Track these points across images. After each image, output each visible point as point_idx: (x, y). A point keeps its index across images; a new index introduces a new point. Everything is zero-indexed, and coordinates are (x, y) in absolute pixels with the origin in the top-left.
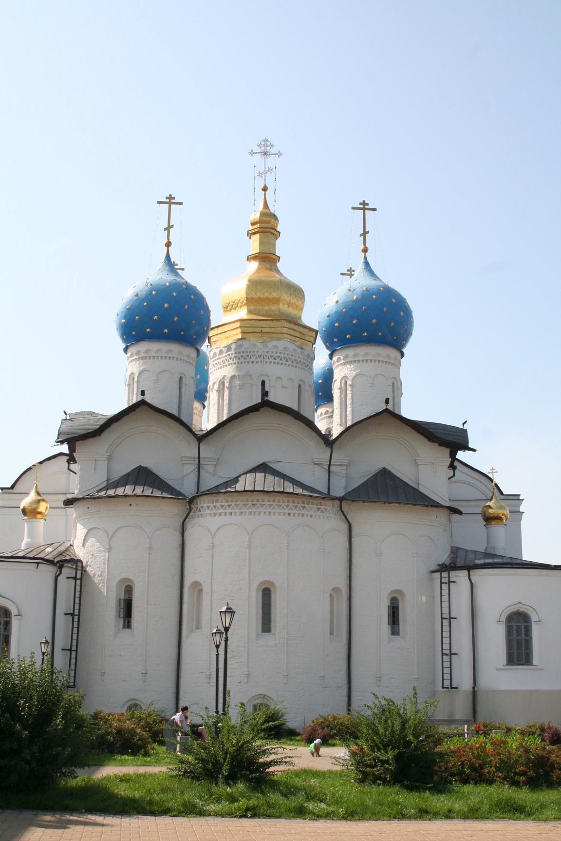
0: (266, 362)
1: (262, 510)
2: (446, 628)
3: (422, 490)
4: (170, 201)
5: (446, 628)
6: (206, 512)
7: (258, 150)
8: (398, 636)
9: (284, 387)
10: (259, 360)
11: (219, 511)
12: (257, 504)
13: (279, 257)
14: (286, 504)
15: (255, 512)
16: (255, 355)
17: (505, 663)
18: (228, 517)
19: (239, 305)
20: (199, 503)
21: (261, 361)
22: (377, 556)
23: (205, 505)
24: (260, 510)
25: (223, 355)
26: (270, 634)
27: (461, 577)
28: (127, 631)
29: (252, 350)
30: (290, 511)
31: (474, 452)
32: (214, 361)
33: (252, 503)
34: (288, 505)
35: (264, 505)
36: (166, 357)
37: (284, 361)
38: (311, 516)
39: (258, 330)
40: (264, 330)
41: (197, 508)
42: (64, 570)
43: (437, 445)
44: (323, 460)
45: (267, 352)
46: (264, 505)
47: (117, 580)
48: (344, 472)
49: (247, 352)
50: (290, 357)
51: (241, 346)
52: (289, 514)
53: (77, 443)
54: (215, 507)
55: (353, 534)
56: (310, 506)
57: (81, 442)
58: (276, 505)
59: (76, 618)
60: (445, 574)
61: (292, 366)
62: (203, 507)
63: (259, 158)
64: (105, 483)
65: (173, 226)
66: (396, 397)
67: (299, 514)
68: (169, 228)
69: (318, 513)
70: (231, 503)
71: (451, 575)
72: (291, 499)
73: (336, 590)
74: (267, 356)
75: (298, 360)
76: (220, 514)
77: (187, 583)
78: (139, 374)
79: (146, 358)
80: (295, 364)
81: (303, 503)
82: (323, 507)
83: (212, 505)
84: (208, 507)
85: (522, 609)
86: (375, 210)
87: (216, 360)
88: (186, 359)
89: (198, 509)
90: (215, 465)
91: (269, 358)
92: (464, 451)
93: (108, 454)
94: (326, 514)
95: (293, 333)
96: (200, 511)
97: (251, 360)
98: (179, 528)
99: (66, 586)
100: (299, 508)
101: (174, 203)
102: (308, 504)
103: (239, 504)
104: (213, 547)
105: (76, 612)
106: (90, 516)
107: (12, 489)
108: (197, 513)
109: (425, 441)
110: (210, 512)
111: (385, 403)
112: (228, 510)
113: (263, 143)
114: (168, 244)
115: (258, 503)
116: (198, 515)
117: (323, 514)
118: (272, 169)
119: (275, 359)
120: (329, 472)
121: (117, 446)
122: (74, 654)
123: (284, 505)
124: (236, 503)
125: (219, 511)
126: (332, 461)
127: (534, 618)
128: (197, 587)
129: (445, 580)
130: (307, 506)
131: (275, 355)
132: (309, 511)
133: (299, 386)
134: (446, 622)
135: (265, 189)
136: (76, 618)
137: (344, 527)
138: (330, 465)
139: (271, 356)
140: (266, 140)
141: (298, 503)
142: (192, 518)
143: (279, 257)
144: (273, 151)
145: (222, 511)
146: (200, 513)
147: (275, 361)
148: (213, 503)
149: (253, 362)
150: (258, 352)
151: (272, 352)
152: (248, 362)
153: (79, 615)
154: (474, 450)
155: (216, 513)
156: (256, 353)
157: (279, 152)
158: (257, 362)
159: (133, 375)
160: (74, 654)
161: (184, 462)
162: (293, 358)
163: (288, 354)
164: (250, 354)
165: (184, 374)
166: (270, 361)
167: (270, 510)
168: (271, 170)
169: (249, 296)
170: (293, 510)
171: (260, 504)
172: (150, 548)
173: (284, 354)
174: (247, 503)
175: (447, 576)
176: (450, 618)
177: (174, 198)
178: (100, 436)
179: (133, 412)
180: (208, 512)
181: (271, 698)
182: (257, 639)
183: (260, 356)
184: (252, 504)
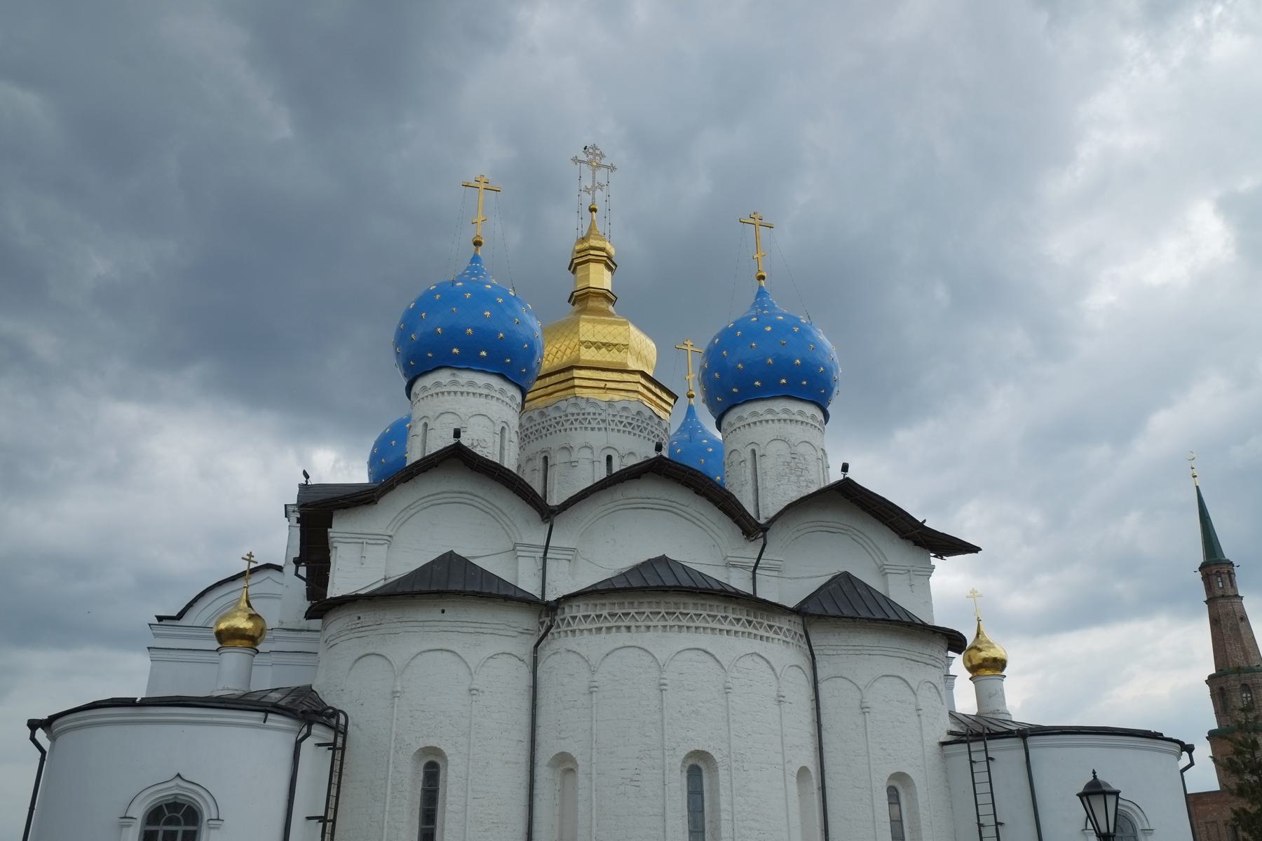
0: (613, 430)
1: (685, 622)
6: (581, 627)
7: (583, 157)
10: (602, 425)
12: (675, 613)
13: (617, 298)
14: (724, 615)
15: (671, 627)
16: (596, 419)
18: (623, 638)
20: (567, 610)
21: (606, 429)
22: (864, 713)
23: (580, 615)
24: (681, 624)
25: (544, 420)
27: (1007, 754)
31: (974, 555)
33: (666, 611)
35: (688, 614)
37: (637, 432)
39: (602, 384)
40: (610, 385)
41: (563, 620)
43: (911, 543)
44: (743, 560)
45: (614, 416)
46: (688, 614)
52: (728, 631)
54: (599, 616)
56: (759, 620)
58: (709, 615)
59: (329, 825)
67: (743, 633)
69: (771, 634)
72: (731, 607)
73: (803, 771)
75: (656, 432)
76: (609, 629)
77: (544, 757)
80: (651, 437)
88: (507, 400)
89: (566, 621)
90: (570, 561)
91: (616, 424)
92: (942, 559)
93: (391, 534)
94: (781, 636)
95: (645, 392)
97: (589, 426)
98: (528, 658)
99: (315, 762)
100: (743, 623)
105: (330, 816)
106: (360, 635)
107: (179, 620)
108: (563, 628)
110: (590, 627)
111: (842, 471)
112: (627, 622)
115: (678, 611)
116: (566, 632)
118: (603, 186)
119: (624, 426)
123: (720, 614)
125: (608, 625)
126: (761, 561)
128: (566, 764)
129: (983, 756)
131: (625, 421)
136: (329, 825)
138: (756, 568)
143: (617, 298)
144: (603, 162)
146: (570, 629)
147: (625, 429)
149: (593, 429)
150: (600, 414)
151: (621, 416)
152: (586, 428)
153: (334, 821)
154: (975, 549)
156: (597, 416)
157: (612, 164)
158: (600, 429)
159: (424, 421)
161: (519, 553)
164: (589, 417)
165: (508, 426)
166: (619, 428)
167: (698, 624)
171: (681, 613)
174: (659, 610)
183: (604, 421)
184: (667, 613)
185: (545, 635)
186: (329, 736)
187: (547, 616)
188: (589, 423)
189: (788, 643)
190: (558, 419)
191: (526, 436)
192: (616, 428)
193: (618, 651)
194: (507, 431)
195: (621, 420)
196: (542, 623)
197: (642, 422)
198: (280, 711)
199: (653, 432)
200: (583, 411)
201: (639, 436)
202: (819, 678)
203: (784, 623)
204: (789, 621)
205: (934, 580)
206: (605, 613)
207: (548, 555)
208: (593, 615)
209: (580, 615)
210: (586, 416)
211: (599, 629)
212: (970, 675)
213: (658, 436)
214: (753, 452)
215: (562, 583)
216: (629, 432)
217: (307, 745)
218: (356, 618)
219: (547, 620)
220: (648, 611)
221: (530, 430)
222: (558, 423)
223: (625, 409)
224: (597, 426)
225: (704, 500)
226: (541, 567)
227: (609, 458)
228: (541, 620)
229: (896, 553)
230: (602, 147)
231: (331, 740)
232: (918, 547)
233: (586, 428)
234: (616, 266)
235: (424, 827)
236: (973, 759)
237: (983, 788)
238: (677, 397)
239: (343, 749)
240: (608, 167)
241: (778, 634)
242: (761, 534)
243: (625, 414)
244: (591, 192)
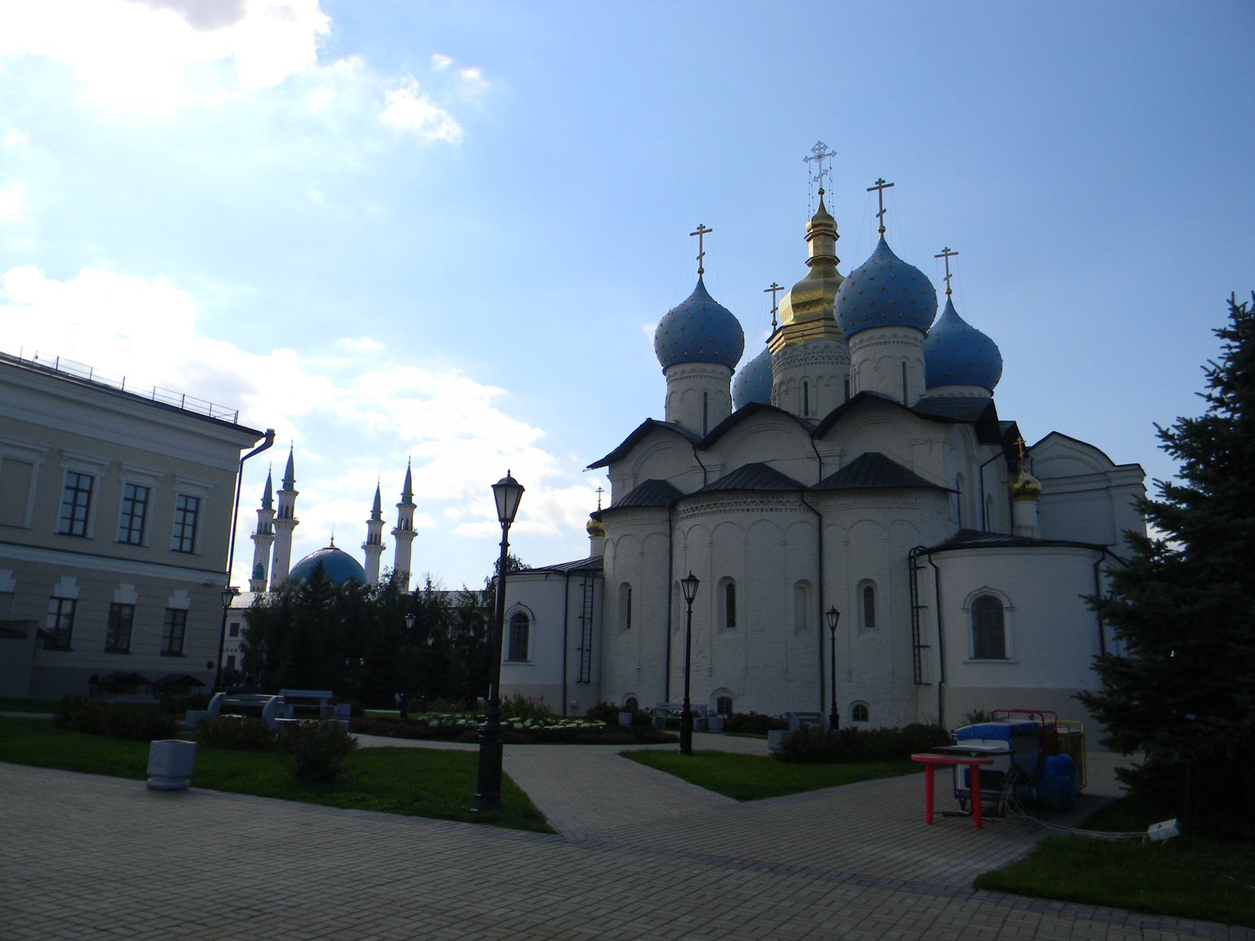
3: (918, 472)
8: (873, 629)
9: (827, 385)
10: (801, 362)
14: (745, 500)
15: (716, 512)
17: (972, 655)
18: (697, 520)
26: (733, 628)
29: (795, 355)
30: (748, 507)
34: (746, 502)
36: (690, 377)
37: (827, 360)
38: (772, 510)
39: (799, 334)
40: (805, 333)
45: (809, 354)
47: (620, 584)
48: (837, 462)
50: (833, 354)
51: (786, 352)
55: (826, 522)
61: (837, 363)
69: (779, 507)
79: (675, 380)
80: (840, 360)
83: (685, 508)
84: (683, 510)
90: (720, 471)
94: (789, 507)
98: (669, 534)
101: (705, 232)
104: (685, 547)
112: (696, 512)
114: (701, 271)
119: (817, 359)
120: (821, 463)
122: (586, 654)
125: (690, 514)
127: (1006, 604)
130: (766, 500)
131: (816, 355)
135: (821, 192)
137: (816, 517)
140: (819, 143)
149: (796, 366)
150: (800, 355)
152: (792, 367)
158: (800, 365)
168: (826, 172)
169: (794, 303)
172: (642, 554)
173: (826, 352)
183: (802, 359)
186: (581, 580)
189: (795, 509)
193: (694, 528)
195: (813, 355)
197: (831, 352)
201: (828, 363)
202: (824, 526)
203: (793, 498)
207: (707, 470)
211: (687, 516)
214: (855, 370)
216: (820, 363)
220: (705, 504)
223: (815, 347)
227: (806, 384)
240: (830, 155)
243: (817, 350)
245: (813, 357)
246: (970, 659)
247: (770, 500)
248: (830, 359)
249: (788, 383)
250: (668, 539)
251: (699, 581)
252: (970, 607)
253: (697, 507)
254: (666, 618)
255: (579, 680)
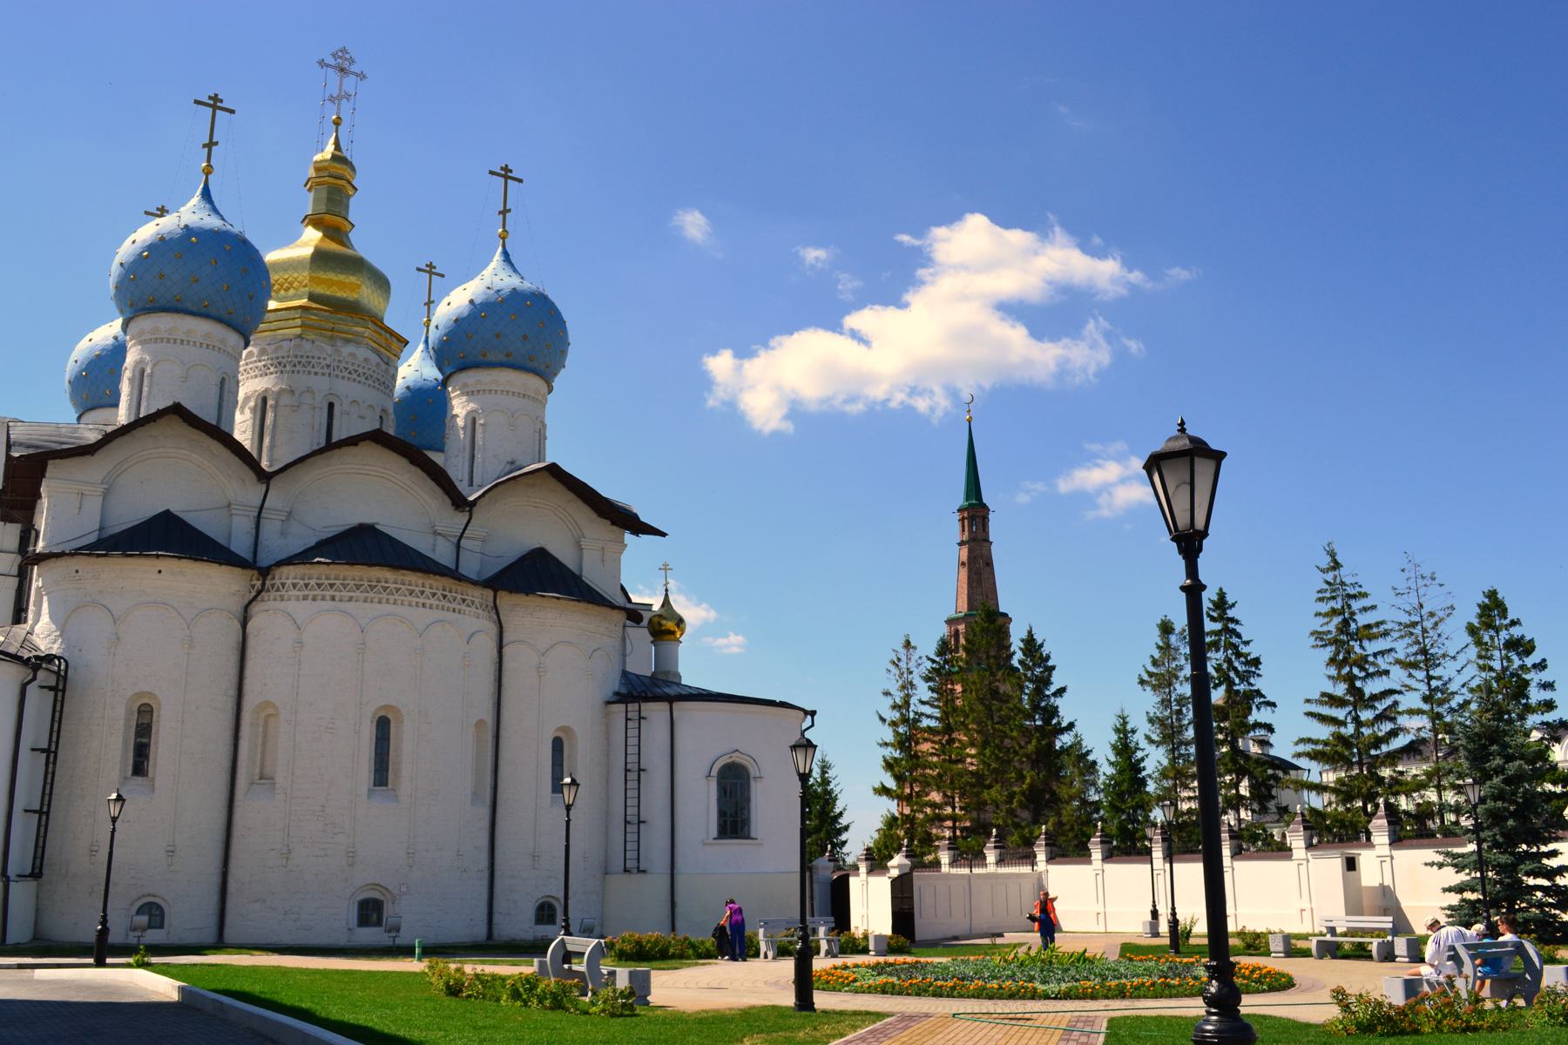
0: (337, 376)
1: (384, 595)
2: (632, 784)
4: (215, 103)
5: (632, 784)
10: (326, 371)
11: (315, 593)
12: (376, 586)
14: (422, 589)
16: (320, 363)
17: (716, 836)
18: (328, 604)
19: (295, 285)
20: (277, 577)
21: (330, 374)
23: (289, 582)
27: (656, 712)
28: (139, 779)
32: (247, 364)
35: (388, 587)
38: (454, 610)
41: (273, 586)
42: (41, 674)
45: (339, 361)
49: (308, 357)
53: (50, 462)
56: (454, 594)
57: (57, 461)
58: (407, 589)
60: (633, 707)
61: (374, 387)
62: (283, 585)
63: (333, 76)
64: (97, 532)
65: (217, 143)
66: (542, 450)
68: (210, 145)
69: (463, 607)
70: (334, 582)
71: (642, 708)
74: (338, 367)
75: (382, 380)
76: (314, 599)
78: (155, 365)
80: (376, 385)
81: (444, 590)
82: (470, 598)
83: (302, 582)
85: (736, 758)
86: (520, 181)
87: (251, 363)
90: (283, 521)
92: (637, 536)
93: (106, 486)
94: (473, 609)
96: (278, 590)
97: (313, 370)
99: (39, 702)
102: (450, 592)
103: (348, 584)
105: (53, 749)
108: (273, 594)
109: (594, 516)
113: (340, 54)
115: (380, 584)
117: (468, 608)
121: (122, 473)
122: (44, 818)
124: (341, 582)
125: (315, 593)
126: (467, 532)
127: (753, 772)
128: (269, 712)
132: (450, 602)
133: (381, 417)
134: (633, 776)
136: (52, 755)
137: (492, 629)
139: (345, 368)
140: (344, 50)
141: (437, 589)
142: (262, 601)
143: (354, 226)
144: (353, 68)
145: (318, 592)
147: (350, 376)
148: (303, 579)
149: (316, 374)
150: (325, 359)
151: (347, 362)
152: (309, 373)
153: (56, 753)
154: (663, 534)
155: (308, 596)
156: (321, 361)
158: (323, 374)
160: (44, 818)
162: (375, 375)
163: (369, 369)
167: (396, 597)
168: (348, 96)
170: (429, 599)
171: (382, 586)
174: (363, 583)
175: (637, 708)
176: (640, 770)
177: (221, 101)
178: (93, 455)
179: (152, 423)
180: (295, 593)
181: (387, 889)
182: (369, 796)
183: (328, 366)
185: (254, 598)
187: (258, 580)
188: (313, 367)
190: (280, 360)
191: (245, 370)
192: (341, 374)
194: (227, 381)
196: (253, 586)
198: (7, 658)
199: (378, 380)
200: (307, 354)
202: (504, 642)
204: (482, 594)
205: (626, 559)
206: (313, 582)
207: (262, 515)
208: (302, 582)
209: (289, 582)
210: (310, 359)
212: (652, 639)
213: (384, 383)
215: (276, 543)
216: (354, 380)
217: (32, 690)
218: (74, 571)
219: (258, 584)
221: (251, 366)
222: (280, 364)
223: (352, 355)
224: (321, 371)
225: (418, 470)
226: (254, 526)
227: (331, 406)
228: (253, 583)
229: (596, 530)
230: (353, 52)
231: (53, 683)
232: (615, 528)
233: (309, 373)
234: (356, 189)
235: (137, 759)
236: (629, 717)
237: (632, 741)
238: (408, 342)
239: (64, 691)
241: (470, 606)
242: (468, 509)
244: (336, 101)
245: (346, 369)
246: (715, 839)
247: (454, 594)
248: (366, 379)
249: (300, 395)
250: (237, 626)
251: (816, 746)
252: (716, 775)
253: (332, 585)
254: (227, 764)
255: (28, 871)
